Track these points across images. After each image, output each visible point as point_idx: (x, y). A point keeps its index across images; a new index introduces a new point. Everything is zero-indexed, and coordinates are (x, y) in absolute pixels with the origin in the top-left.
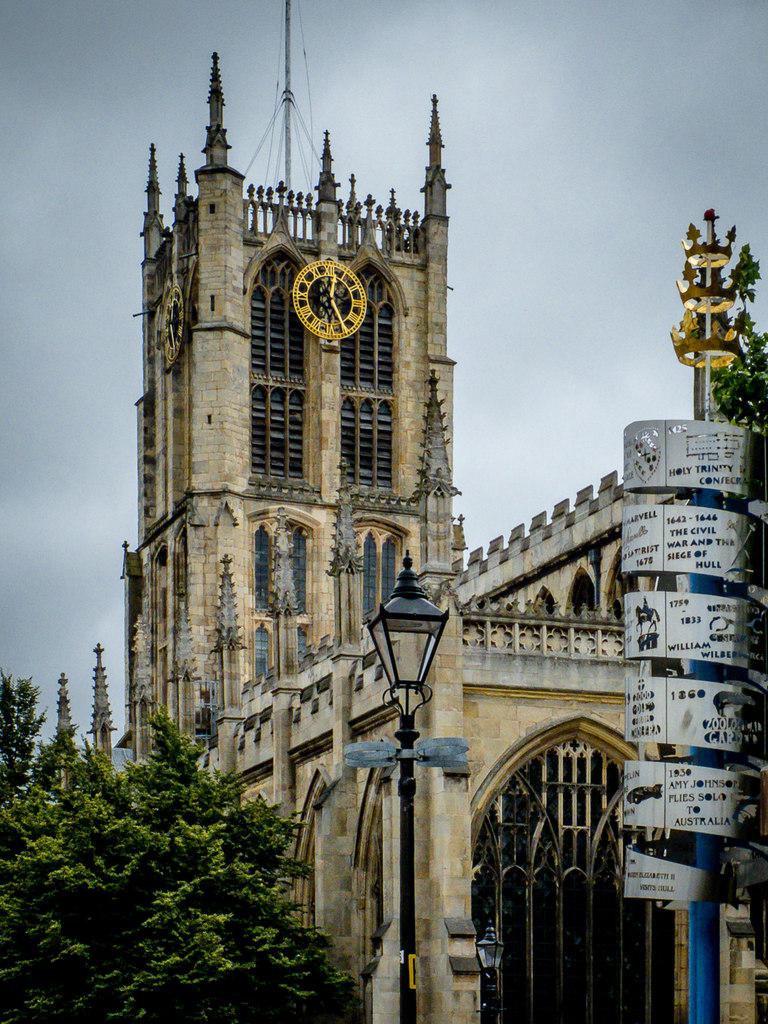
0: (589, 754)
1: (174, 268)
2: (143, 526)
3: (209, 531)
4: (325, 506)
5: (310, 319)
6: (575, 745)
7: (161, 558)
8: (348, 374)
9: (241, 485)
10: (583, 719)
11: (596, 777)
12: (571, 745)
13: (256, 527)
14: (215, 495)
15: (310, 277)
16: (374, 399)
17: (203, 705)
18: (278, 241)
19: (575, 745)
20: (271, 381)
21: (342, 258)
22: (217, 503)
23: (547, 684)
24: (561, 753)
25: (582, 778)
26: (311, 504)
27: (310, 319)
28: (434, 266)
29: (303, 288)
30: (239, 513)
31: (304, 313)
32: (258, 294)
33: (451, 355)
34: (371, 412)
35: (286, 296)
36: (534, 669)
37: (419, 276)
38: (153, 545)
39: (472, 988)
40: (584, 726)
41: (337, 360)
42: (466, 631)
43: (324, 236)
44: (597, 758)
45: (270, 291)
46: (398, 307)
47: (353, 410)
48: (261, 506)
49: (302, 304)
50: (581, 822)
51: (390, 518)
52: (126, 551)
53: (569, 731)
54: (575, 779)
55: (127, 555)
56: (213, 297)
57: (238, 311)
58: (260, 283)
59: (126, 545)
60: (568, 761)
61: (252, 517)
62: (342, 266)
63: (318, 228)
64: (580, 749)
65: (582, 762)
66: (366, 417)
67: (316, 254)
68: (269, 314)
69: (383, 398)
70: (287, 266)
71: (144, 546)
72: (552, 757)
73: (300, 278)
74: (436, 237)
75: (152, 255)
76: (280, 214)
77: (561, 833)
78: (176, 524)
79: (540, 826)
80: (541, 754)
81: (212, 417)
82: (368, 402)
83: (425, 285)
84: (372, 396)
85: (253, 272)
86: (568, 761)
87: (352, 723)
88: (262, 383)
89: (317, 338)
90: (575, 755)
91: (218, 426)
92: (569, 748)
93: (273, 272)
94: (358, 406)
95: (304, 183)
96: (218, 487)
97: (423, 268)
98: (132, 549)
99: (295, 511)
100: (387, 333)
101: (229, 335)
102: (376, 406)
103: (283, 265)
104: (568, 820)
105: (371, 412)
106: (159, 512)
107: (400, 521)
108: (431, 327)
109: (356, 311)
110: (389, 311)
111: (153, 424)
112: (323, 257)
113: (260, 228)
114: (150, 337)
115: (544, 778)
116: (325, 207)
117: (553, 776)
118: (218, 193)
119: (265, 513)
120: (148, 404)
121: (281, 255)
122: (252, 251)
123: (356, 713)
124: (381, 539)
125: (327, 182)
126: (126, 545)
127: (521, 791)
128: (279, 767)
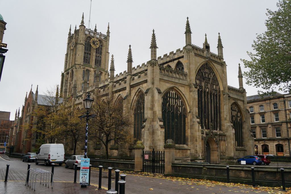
0: (174, 92)
1: (74, 38)
4: (92, 68)
6: (173, 91)
7: (68, 74)
8: (96, 52)
9: (82, 64)
13: (83, 70)
14: (79, 65)
18: (89, 35)
19: (173, 91)
20: (87, 52)
21: (97, 39)
22: (79, 66)
23: (170, 80)
26: (91, 68)
28: (107, 41)
29: (92, 41)
30: (82, 67)
31: (92, 44)
32: (86, 41)
33: (109, 52)
35: (90, 42)
36: (168, 77)
40: (175, 88)
41: (95, 50)
43: (95, 36)
44: (175, 93)
47: (96, 57)
49: (92, 43)
50: (173, 104)
53: (172, 88)
57: (84, 43)
61: (83, 68)
63: (94, 35)
64: (173, 92)
65: (173, 94)
73: (92, 40)
76: (90, 32)
77: (171, 105)
78: (71, 69)
79: (168, 104)
82: (98, 56)
83: (106, 44)
85: (86, 38)
87: (131, 86)
89: (93, 47)
90: (173, 92)
95: (93, 29)
96: (79, 64)
99: (89, 68)
100: (101, 49)
101: (82, 45)
102: (99, 57)
104: (172, 103)
106: (67, 68)
107: (102, 71)
108: (107, 48)
109: (98, 45)
110: (102, 46)
115: (168, 96)
119: (85, 68)
120: (67, 55)
121: (89, 37)
122: (86, 36)
123: (132, 84)
125: (96, 30)
128: (128, 89)
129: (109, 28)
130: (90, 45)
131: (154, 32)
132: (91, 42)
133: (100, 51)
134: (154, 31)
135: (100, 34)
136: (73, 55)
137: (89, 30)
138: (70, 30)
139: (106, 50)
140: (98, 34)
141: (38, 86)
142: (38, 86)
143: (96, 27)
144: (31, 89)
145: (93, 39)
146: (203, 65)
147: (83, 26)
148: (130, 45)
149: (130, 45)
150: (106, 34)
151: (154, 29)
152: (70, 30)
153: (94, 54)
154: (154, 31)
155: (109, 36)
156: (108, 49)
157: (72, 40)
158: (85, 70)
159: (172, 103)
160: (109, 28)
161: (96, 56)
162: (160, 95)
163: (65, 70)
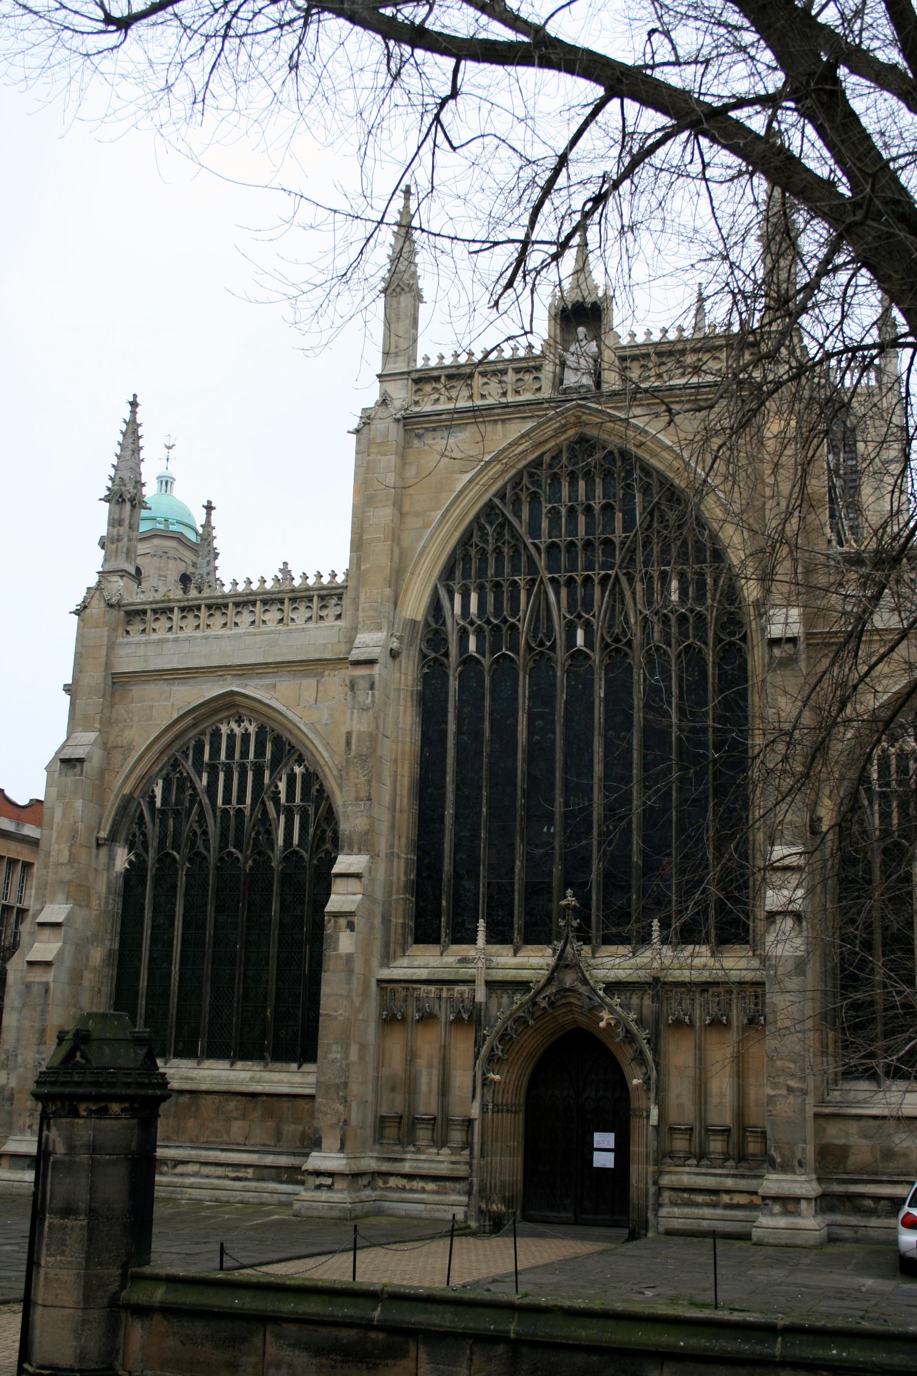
0: (252, 729)
10: (232, 693)
11: (260, 753)
12: (236, 721)
19: (239, 721)
24: (224, 729)
25: (245, 754)
39: (44, 980)
42: (128, 623)
44: (261, 730)
54: (237, 755)
60: (231, 736)
64: (246, 724)
65: (246, 736)
72: (216, 735)
80: (203, 733)
86: (231, 736)
90: (238, 731)
92: (234, 725)
115: (206, 757)
117: (215, 752)
127: (181, 774)
131: (134, 413)
134: (134, 404)
146: (537, 463)
148: (209, 502)
149: (209, 502)
151: (135, 396)
154: (134, 404)
159: (227, 800)
162: (71, 773)
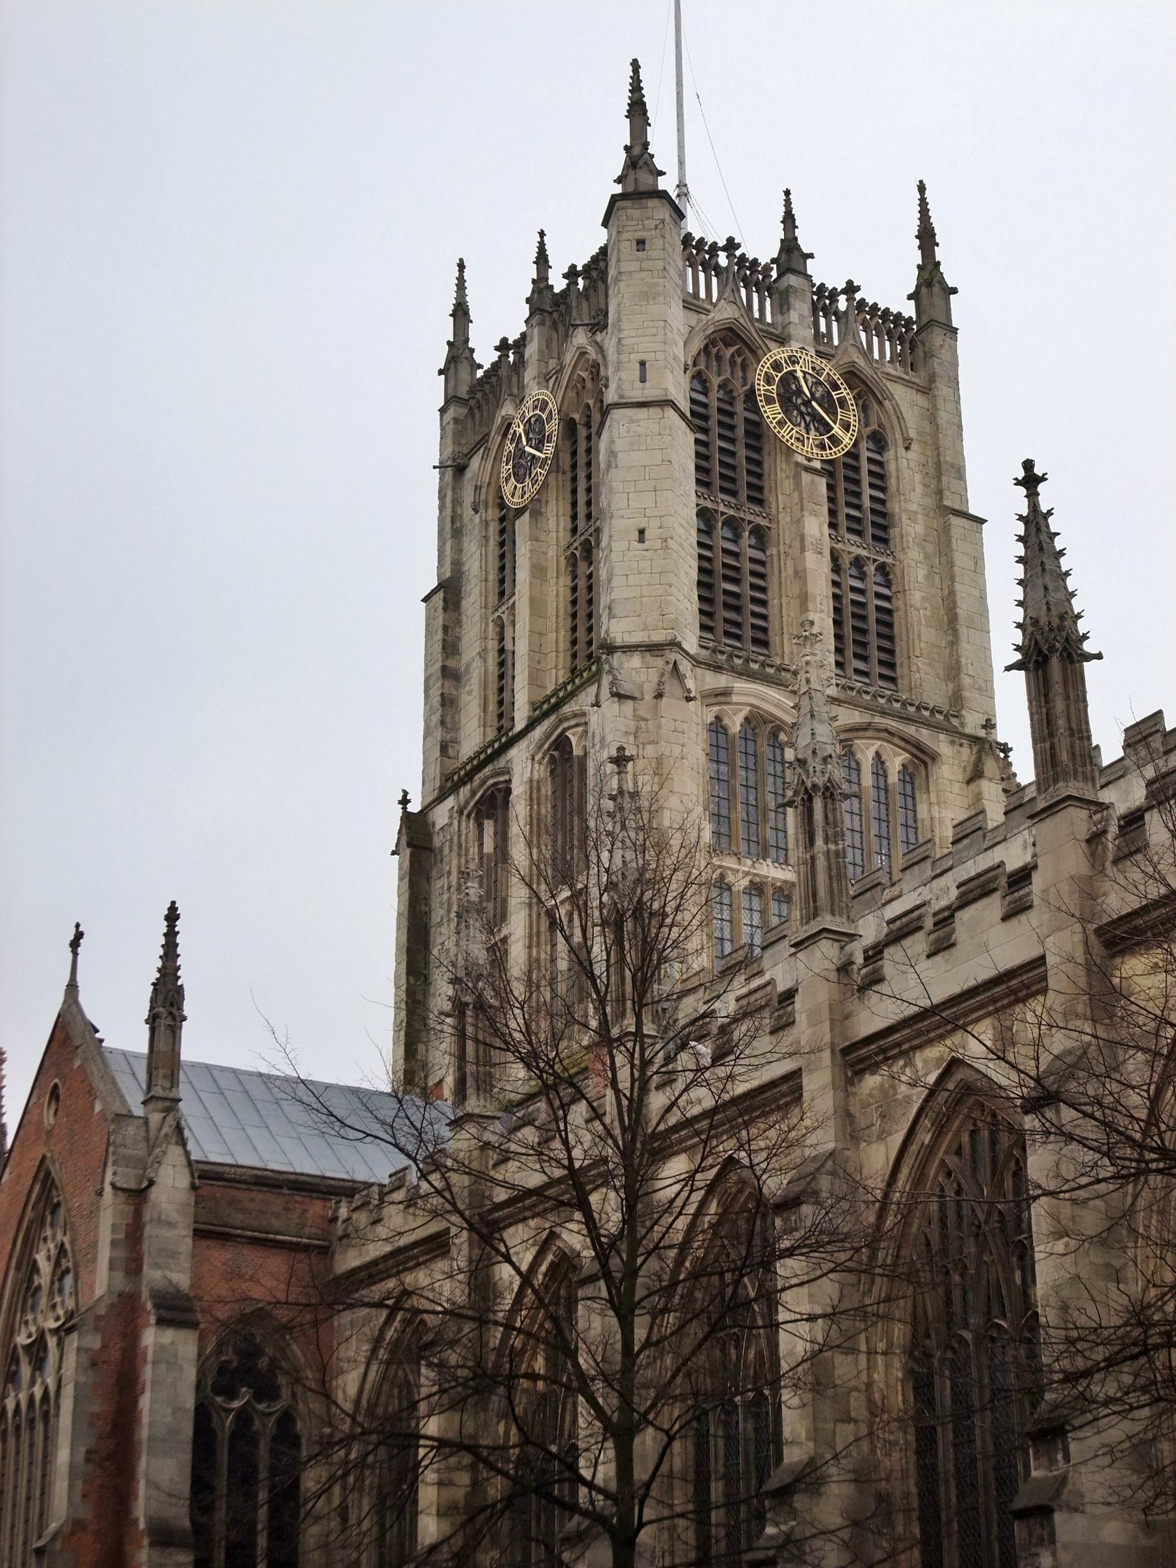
2: (435, 771)
3: (644, 709)
5: (781, 423)
9: (691, 641)
14: (653, 649)
15: (777, 366)
16: (868, 558)
17: (121, 1281)
20: (723, 506)
22: (659, 662)
27: (781, 423)
28: (942, 389)
29: (769, 380)
31: (772, 413)
34: (862, 577)
35: (740, 391)
37: (920, 399)
38: (465, 791)
41: (822, 483)
45: (716, 381)
46: (895, 437)
48: (722, 681)
49: (769, 400)
51: (910, 730)
52: (404, 809)
55: (407, 817)
56: (643, 364)
57: (679, 389)
58: (702, 366)
59: (404, 801)
62: (820, 363)
66: (858, 584)
67: (782, 341)
68: (714, 412)
69: (882, 559)
70: (739, 353)
71: (439, 799)
74: (943, 351)
75: (463, 392)
78: (538, 733)
81: (647, 533)
83: (932, 416)
84: (864, 553)
88: (709, 505)
89: (790, 451)
91: (658, 544)
93: (719, 358)
94: (846, 561)
96: (659, 637)
97: (927, 390)
98: (414, 807)
102: (871, 569)
103: (732, 349)
105: (862, 577)
107: (924, 735)
110: (879, 441)
111: (459, 623)
112: (795, 346)
113: (703, 295)
114: (457, 502)
116: (792, 280)
118: (650, 224)
121: (729, 335)
122: (693, 318)
124: (896, 761)
126: (404, 801)
129: (927, 237)
130: (756, 431)
132: (761, 387)
133: (867, 503)
135: (842, 304)
136: (538, 571)
137: (723, 259)
138: (461, 313)
139: (940, 493)
140: (823, 300)
141: (922, 188)
142: (172, 916)
143: (789, 220)
144: (72, 988)
145: (778, 353)
147: (653, 203)
150: (909, 310)
152: (461, 313)
153: (816, 526)
155: (954, 331)
156: (960, 473)
157: (507, 409)
158: (735, 724)
160: (927, 237)
161: (835, 557)
163: (447, 778)
